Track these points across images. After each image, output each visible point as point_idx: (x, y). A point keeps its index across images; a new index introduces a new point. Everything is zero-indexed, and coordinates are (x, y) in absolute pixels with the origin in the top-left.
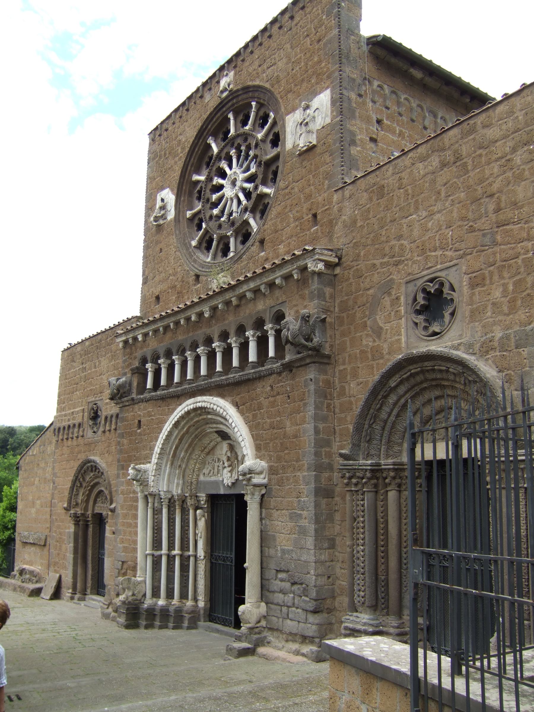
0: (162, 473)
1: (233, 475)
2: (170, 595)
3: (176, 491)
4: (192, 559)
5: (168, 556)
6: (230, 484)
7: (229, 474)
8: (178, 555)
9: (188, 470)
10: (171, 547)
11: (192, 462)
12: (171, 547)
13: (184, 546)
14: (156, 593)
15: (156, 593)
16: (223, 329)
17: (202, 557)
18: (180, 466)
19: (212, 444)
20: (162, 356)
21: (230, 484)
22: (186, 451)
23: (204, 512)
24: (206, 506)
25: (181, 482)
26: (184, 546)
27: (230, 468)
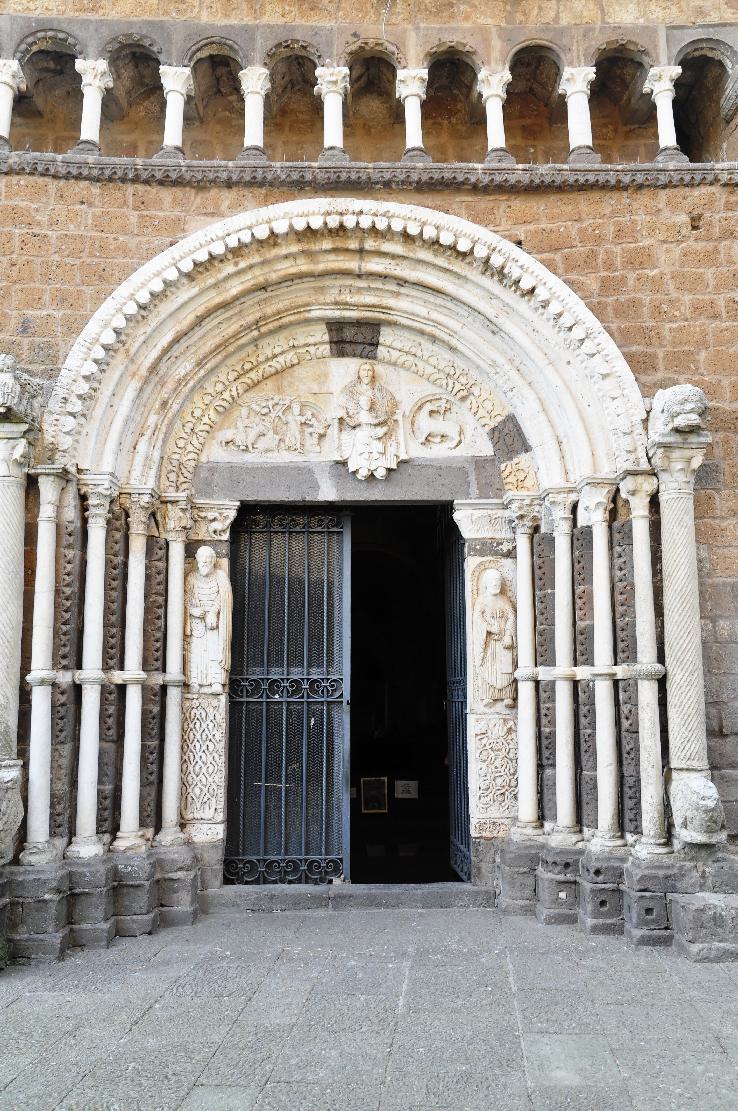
0: (98, 412)
1: (391, 450)
2: (109, 821)
3: (142, 482)
4: (174, 695)
5: (105, 690)
6: (380, 473)
7: (378, 446)
8: (137, 682)
9: (178, 425)
10: (114, 655)
11: (199, 401)
12: (114, 655)
13: (154, 658)
14: (64, 823)
15: (64, 823)
16: (452, 38)
17: (218, 688)
18: (164, 404)
19: (291, 357)
20: (92, 50)
21: (380, 473)
22: (200, 364)
23: (219, 555)
24: (226, 536)
25: (156, 455)
26: (154, 658)
27: (381, 431)
